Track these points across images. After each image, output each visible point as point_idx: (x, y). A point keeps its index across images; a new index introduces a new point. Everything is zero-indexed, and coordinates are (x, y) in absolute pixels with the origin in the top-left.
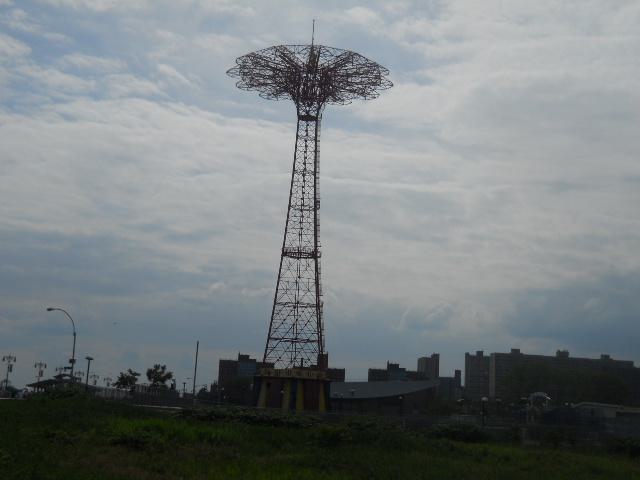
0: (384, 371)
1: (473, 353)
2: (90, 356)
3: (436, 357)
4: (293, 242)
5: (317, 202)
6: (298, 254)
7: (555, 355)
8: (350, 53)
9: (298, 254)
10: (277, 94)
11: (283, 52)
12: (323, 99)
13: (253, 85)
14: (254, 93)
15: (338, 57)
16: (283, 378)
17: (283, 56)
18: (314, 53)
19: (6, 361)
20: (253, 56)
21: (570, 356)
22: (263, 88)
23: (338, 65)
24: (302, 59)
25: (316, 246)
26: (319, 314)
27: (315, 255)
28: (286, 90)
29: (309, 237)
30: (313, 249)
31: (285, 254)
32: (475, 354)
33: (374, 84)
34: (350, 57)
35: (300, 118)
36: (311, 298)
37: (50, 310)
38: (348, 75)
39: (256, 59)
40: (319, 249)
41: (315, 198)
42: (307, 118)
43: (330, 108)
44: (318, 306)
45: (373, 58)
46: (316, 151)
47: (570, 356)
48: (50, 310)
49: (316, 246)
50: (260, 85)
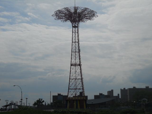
0: (98, 95)
1: (123, 89)
2: (27, 98)
3: (112, 91)
4: (73, 62)
5: (79, 50)
6: (75, 65)
7: (145, 88)
8: (86, 8)
9: (75, 65)
10: (66, 21)
11: (67, 9)
12: (79, 21)
13: (59, 19)
14: (60, 21)
15: (82, 9)
16: (74, 100)
17: (67, 10)
18: (76, 9)
19: (6, 101)
20: (59, 11)
22: (62, 19)
23: (82, 12)
24: (73, 11)
25: (80, 62)
26: (82, 81)
27: (80, 65)
28: (68, 19)
30: (78, 63)
31: (71, 65)
32: (123, 89)
33: (93, 16)
34: (86, 9)
35: (73, 27)
36: (80, 77)
37: (14, 86)
38: (85, 14)
39: (60, 11)
40: (81, 63)
42: (75, 27)
43: (81, 24)
44: (82, 79)
45: (92, 9)
46: (78, 36)
47: (149, 87)
48: (14, 86)
50: (61, 18)
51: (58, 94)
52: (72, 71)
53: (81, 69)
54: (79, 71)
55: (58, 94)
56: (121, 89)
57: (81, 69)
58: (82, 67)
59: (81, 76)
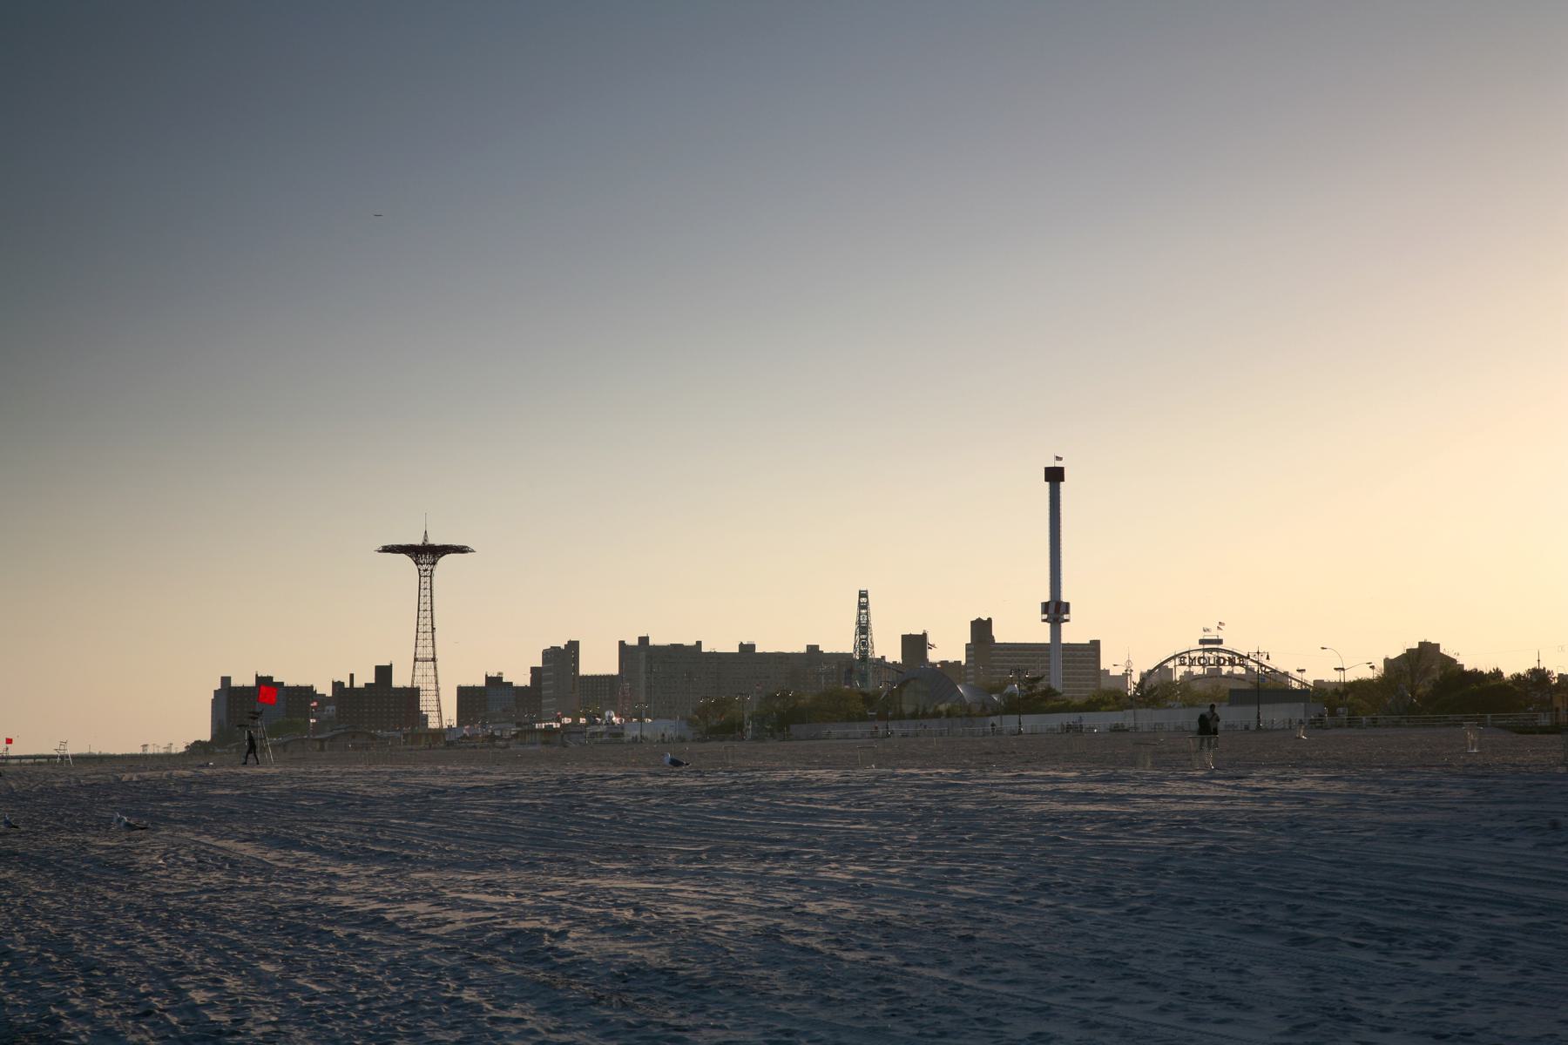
0: (480, 688)
1: (633, 641)
3: (573, 646)
5: (433, 629)
7: (736, 650)
12: (434, 563)
21: (758, 650)
25: (434, 654)
26: (437, 695)
27: (434, 660)
29: (430, 649)
31: (416, 660)
32: (635, 642)
41: (432, 625)
44: (437, 690)
47: (758, 650)
49: (434, 654)
51: (259, 679)
52: (418, 673)
53: (435, 668)
54: (431, 672)
55: (259, 679)
56: (622, 643)
57: (435, 668)
58: (438, 663)
59: (437, 683)
